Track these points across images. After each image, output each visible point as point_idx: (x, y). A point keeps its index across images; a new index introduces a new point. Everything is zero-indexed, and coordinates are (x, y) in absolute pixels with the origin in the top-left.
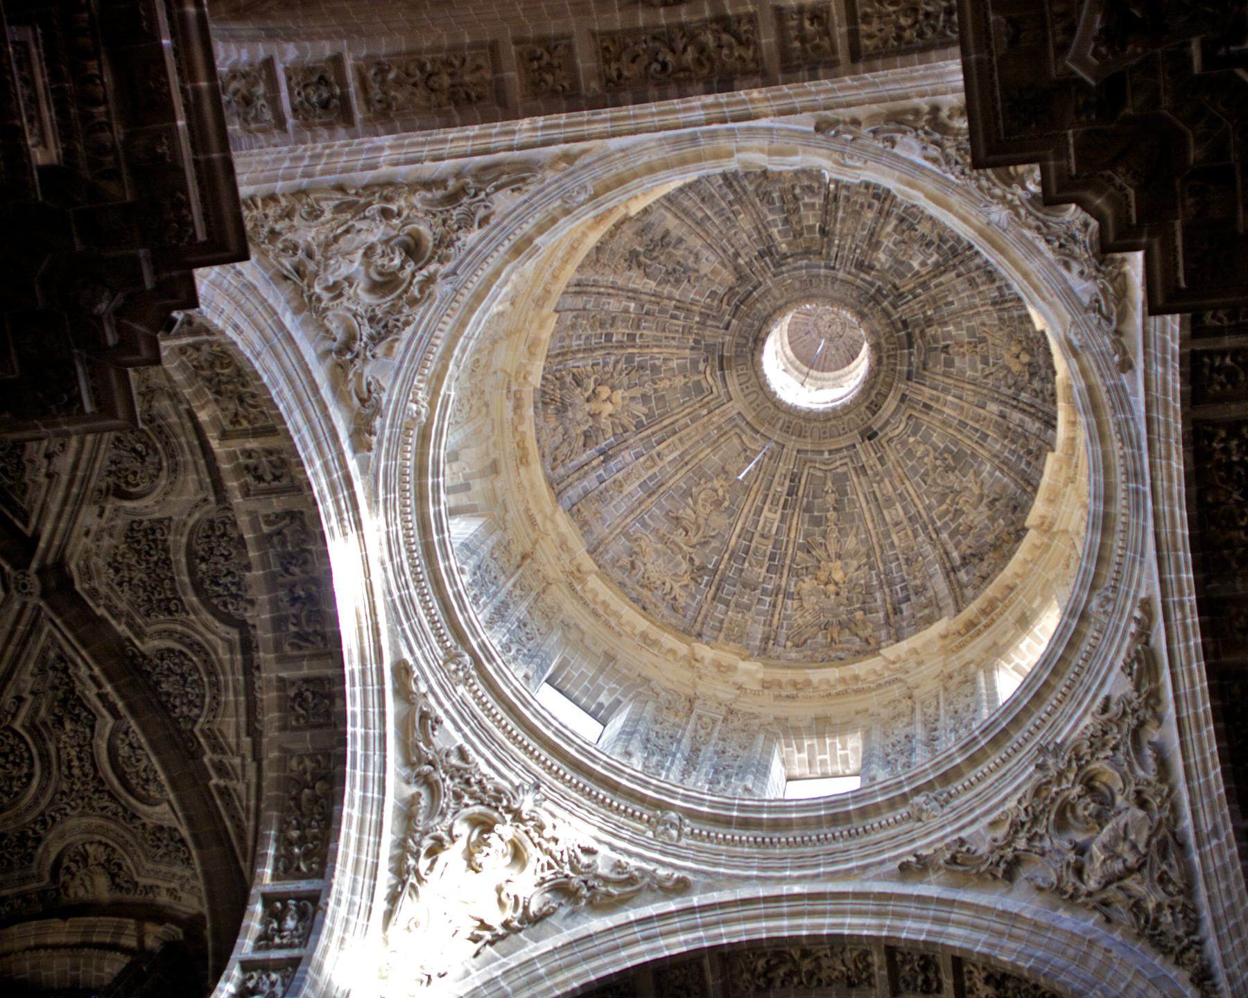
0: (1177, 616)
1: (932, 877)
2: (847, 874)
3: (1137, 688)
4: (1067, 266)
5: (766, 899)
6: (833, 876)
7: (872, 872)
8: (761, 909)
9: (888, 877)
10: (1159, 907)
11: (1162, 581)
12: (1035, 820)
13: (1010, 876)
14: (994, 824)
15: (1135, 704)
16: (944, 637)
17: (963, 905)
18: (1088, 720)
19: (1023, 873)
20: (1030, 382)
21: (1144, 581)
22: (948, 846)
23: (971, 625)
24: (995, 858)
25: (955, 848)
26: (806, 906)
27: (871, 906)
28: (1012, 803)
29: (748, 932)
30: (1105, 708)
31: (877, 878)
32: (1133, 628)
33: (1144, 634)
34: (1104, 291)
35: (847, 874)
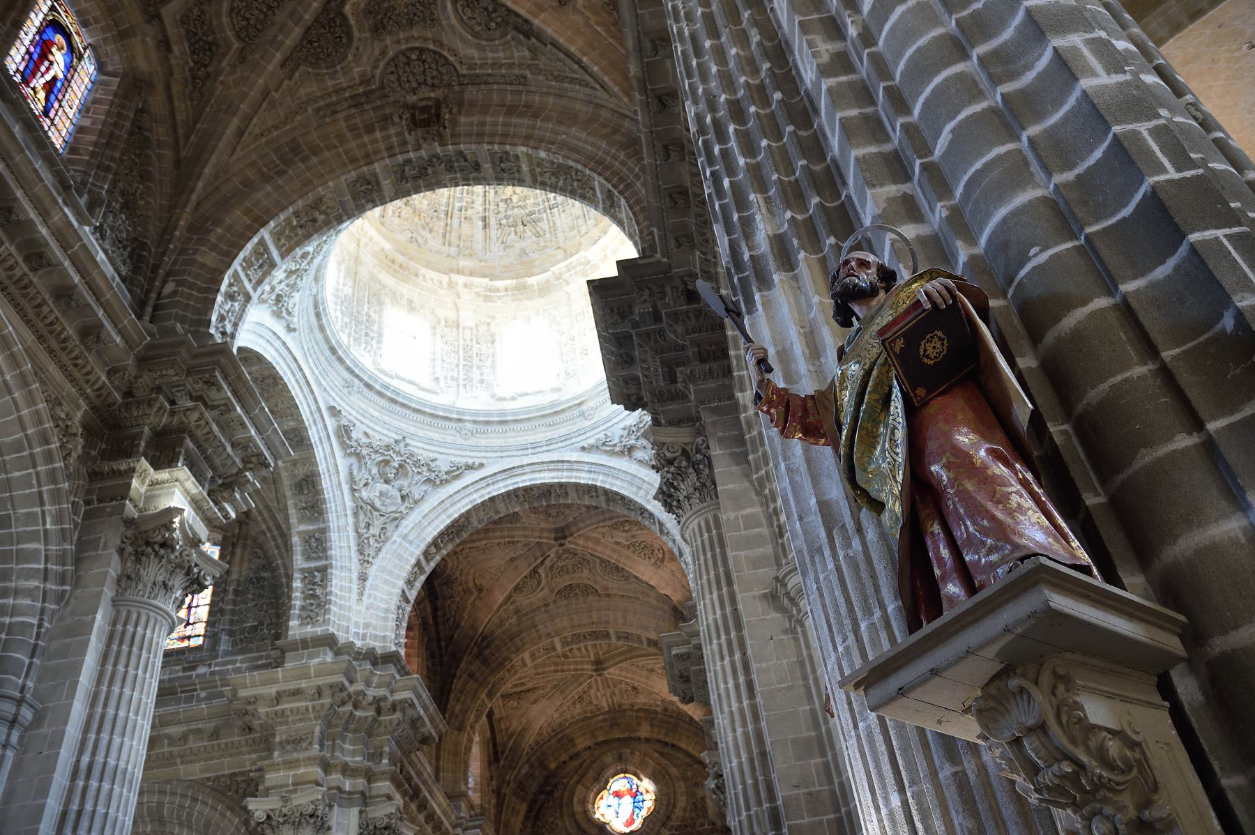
0: (483, 483)
1: (333, 420)
2: (320, 385)
3: (446, 473)
4: (624, 429)
5: (299, 366)
6: (317, 380)
7: (325, 394)
8: (294, 366)
9: (326, 402)
10: (374, 536)
11: (495, 474)
12: (377, 452)
13: (350, 455)
14: (366, 434)
15: (440, 475)
16: (382, 250)
17: (331, 446)
18: (425, 454)
19: (353, 460)
20: (502, 200)
21: (491, 460)
22: (349, 421)
23: (393, 262)
24: (354, 444)
25: (351, 424)
26: (302, 382)
27: (313, 407)
28: (378, 437)
29: (285, 373)
30: (432, 461)
31: (324, 398)
32: (470, 461)
33: (470, 467)
34: (615, 445)
35: (320, 385)
